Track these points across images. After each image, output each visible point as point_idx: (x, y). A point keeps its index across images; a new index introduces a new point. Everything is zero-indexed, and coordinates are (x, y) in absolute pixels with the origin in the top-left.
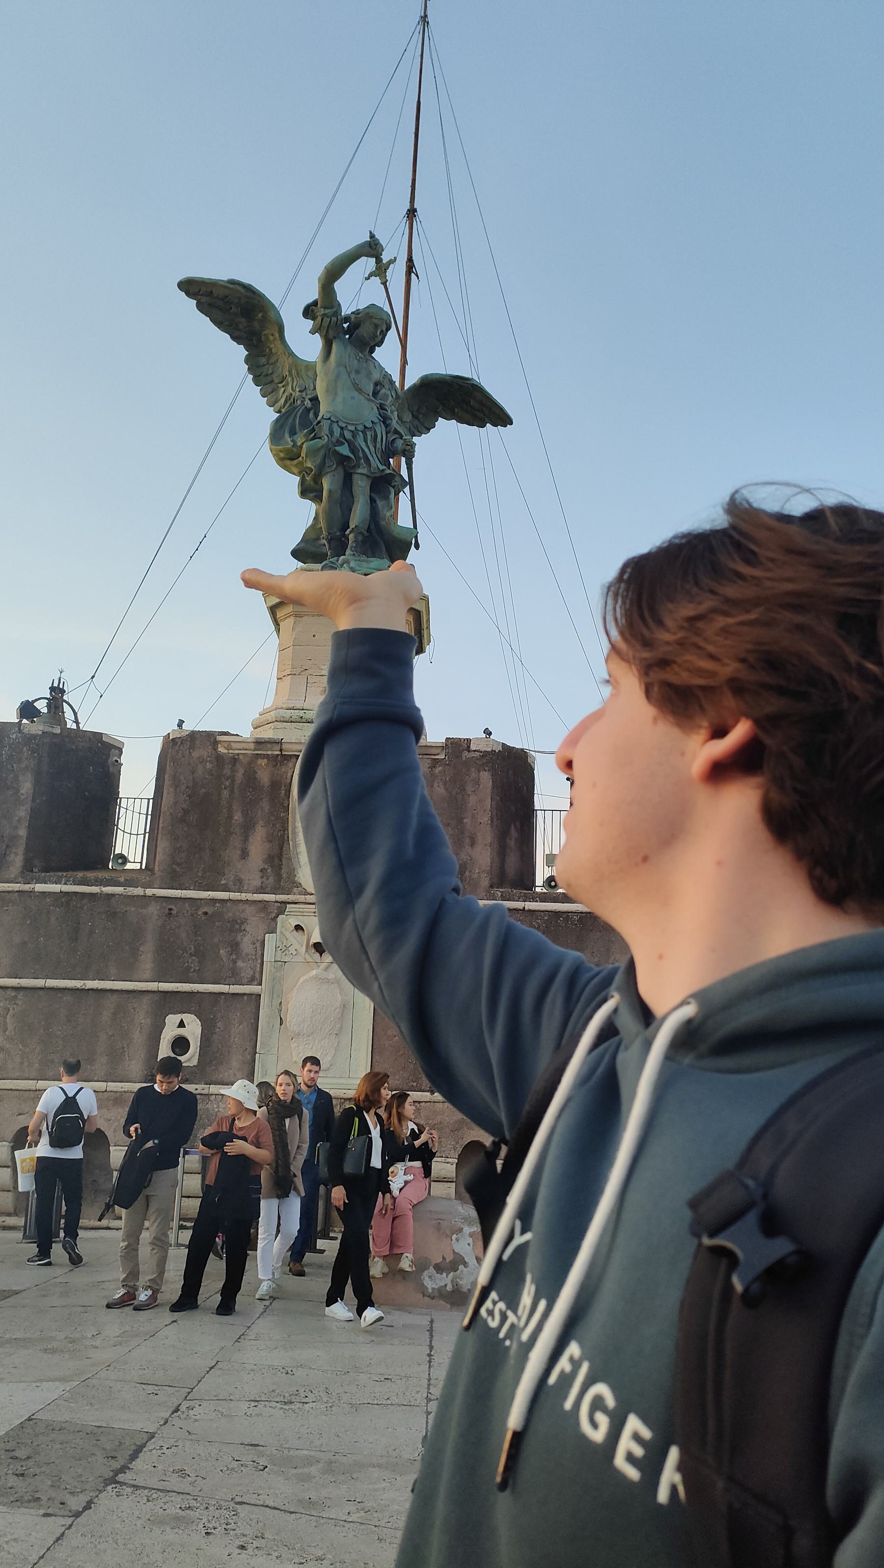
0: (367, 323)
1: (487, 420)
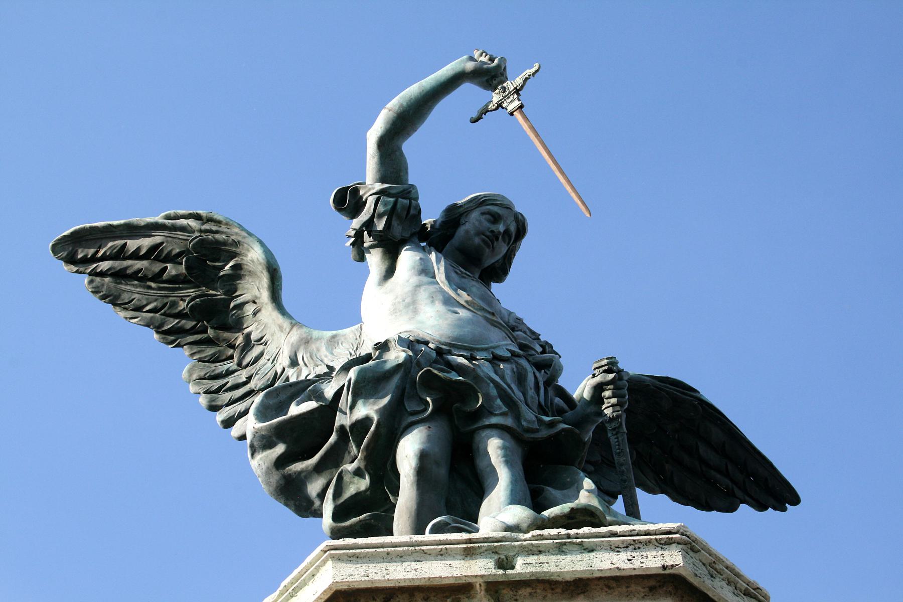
0: (475, 215)
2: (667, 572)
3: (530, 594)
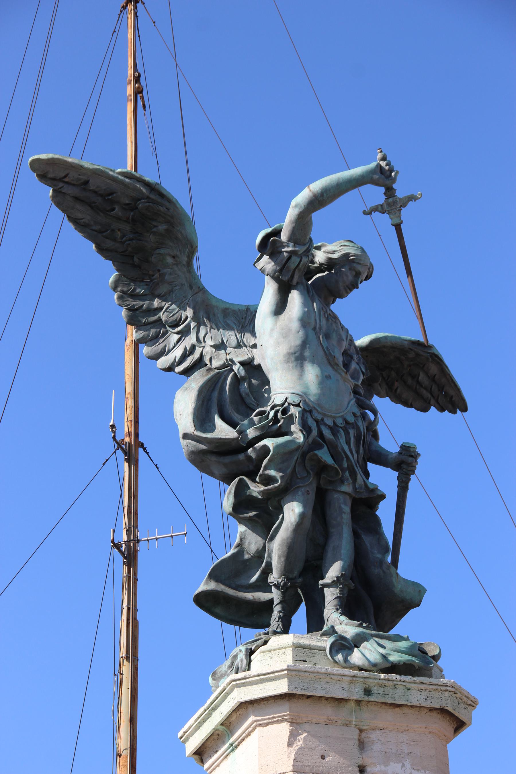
1: (433, 401)
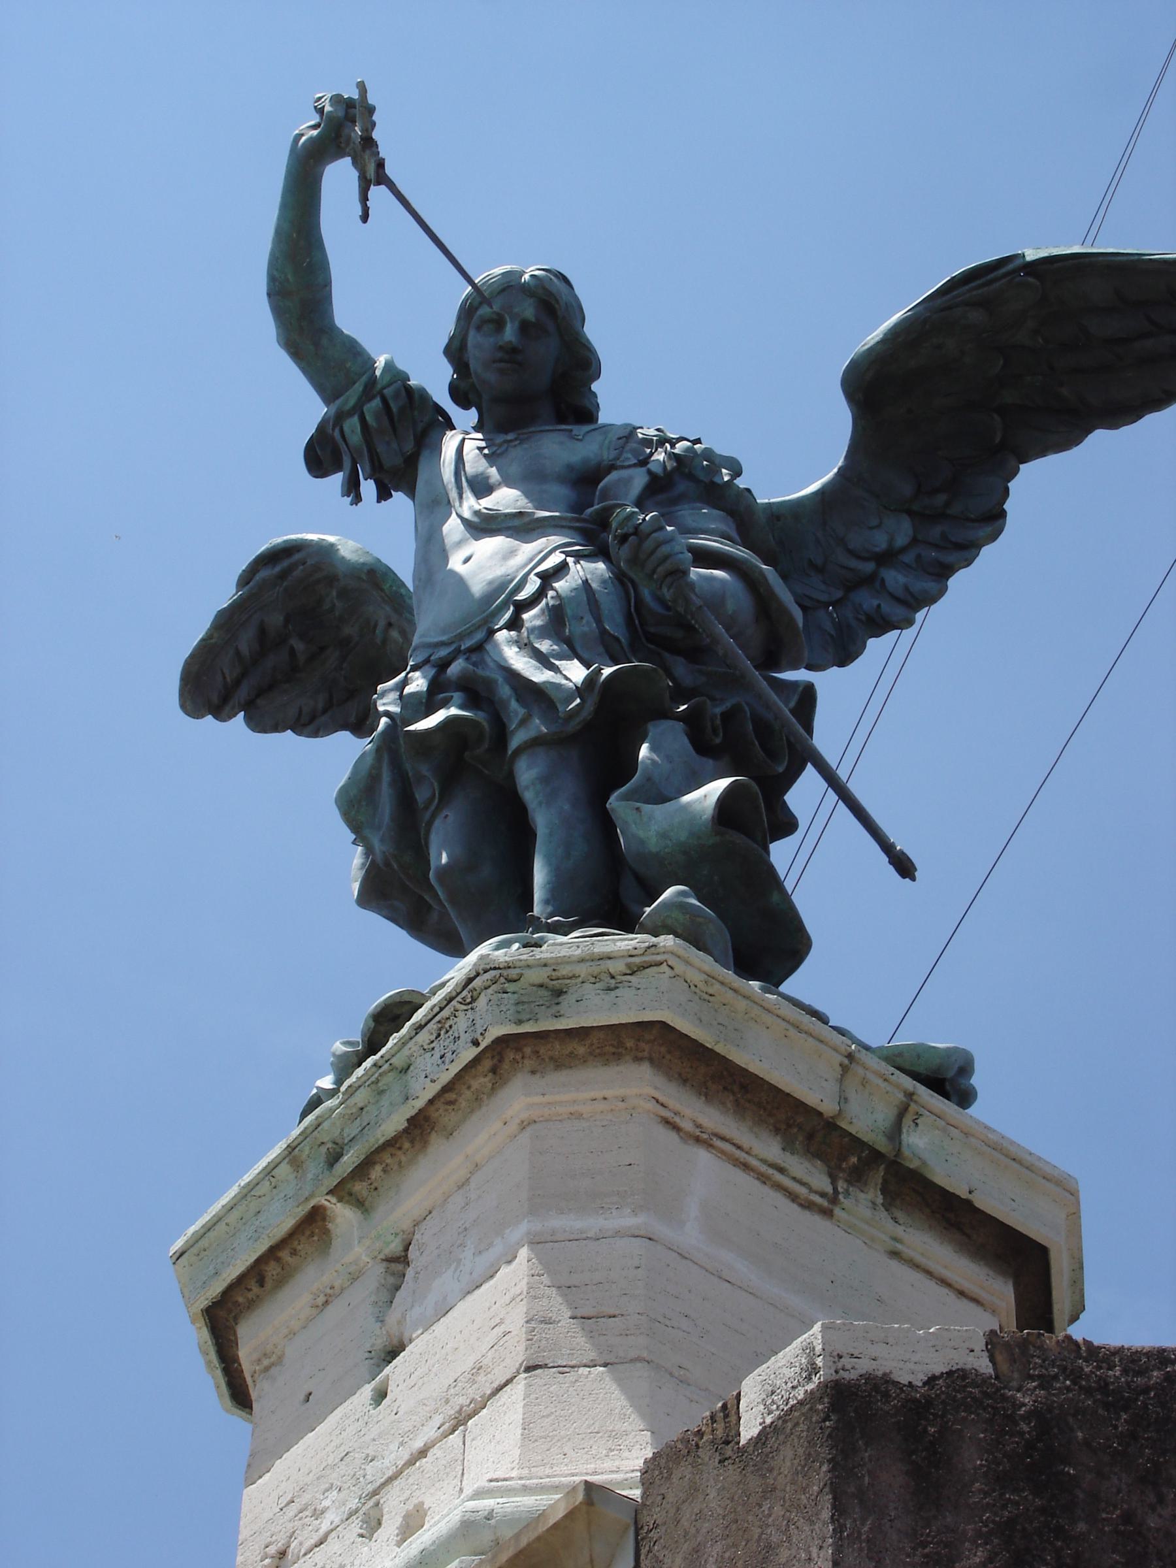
0: (473, 338)
2: (483, 1045)
3: (384, 1171)
